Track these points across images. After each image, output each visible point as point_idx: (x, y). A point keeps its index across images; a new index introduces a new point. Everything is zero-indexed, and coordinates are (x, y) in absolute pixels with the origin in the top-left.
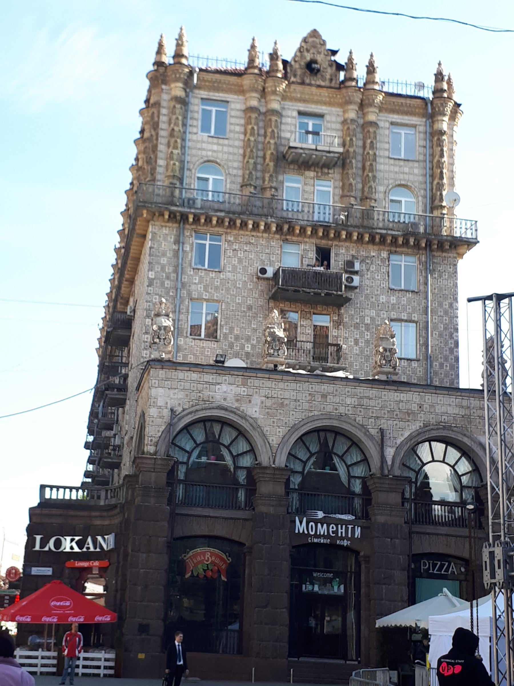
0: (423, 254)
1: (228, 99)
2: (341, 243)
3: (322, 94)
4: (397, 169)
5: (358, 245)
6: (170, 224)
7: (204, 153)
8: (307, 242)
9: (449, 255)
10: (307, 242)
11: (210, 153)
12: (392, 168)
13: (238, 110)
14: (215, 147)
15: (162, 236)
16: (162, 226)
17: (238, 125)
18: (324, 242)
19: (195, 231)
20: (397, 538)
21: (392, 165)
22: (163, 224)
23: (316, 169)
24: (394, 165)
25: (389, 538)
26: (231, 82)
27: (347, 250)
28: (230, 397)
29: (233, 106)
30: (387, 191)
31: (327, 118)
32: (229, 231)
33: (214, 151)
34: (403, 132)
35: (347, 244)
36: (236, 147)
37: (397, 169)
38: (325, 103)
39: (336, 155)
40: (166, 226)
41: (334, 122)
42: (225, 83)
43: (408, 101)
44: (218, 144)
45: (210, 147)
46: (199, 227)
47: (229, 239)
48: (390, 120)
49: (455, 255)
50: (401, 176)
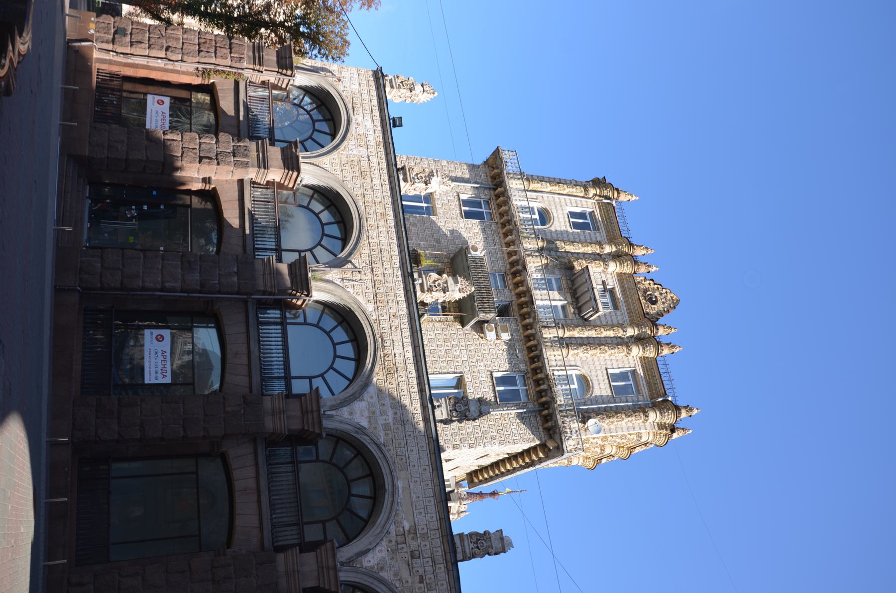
0: (534, 405)
1: (601, 230)
2: (520, 324)
3: (635, 305)
4: (600, 378)
5: (523, 341)
6: (489, 179)
7: (554, 211)
8: (511, 293)
9: (542, 433)
10: (511, 293)
11: (555, 215)
12: (599, 373)
13: (596, 238)
14: (562, 220)
15: (478, 173)
16: (486, 173)
17: (585, 238)
18: (516, 308)
19: (490, 199)
20: (238, 279)
21: (602, 372)
22: (488, 174)
23: (574, 303)
24: (603, 374)
25: (238, 269)
26: (614, 231)
27: (515, 331)
28: (361, 130)
29: (598, 234)
30: (579, 368)
31: (618, 313)
32: (500, 226)
33: (558, 218)
34: (631, 382)
35: (521, 330)
36: (568, 236)
37: (600, 378)
38: (629, 309)
39: (595, 307)
40: (487, 176)
41: (617, 318)
42: (612, 227)
43: (659, 381)
44: (565, 221)
45: (561, 216)
46: (494, 201)
47: (493, 226)
48: (637, 368)
49: (543, 439)
50: (595, 382)
